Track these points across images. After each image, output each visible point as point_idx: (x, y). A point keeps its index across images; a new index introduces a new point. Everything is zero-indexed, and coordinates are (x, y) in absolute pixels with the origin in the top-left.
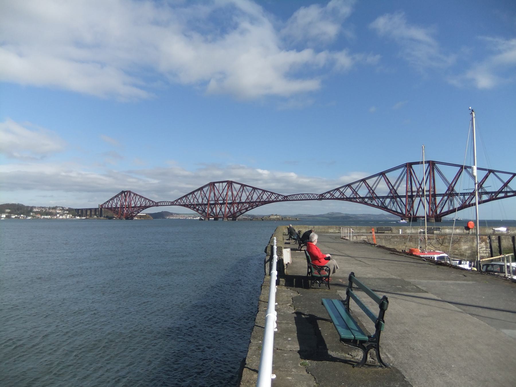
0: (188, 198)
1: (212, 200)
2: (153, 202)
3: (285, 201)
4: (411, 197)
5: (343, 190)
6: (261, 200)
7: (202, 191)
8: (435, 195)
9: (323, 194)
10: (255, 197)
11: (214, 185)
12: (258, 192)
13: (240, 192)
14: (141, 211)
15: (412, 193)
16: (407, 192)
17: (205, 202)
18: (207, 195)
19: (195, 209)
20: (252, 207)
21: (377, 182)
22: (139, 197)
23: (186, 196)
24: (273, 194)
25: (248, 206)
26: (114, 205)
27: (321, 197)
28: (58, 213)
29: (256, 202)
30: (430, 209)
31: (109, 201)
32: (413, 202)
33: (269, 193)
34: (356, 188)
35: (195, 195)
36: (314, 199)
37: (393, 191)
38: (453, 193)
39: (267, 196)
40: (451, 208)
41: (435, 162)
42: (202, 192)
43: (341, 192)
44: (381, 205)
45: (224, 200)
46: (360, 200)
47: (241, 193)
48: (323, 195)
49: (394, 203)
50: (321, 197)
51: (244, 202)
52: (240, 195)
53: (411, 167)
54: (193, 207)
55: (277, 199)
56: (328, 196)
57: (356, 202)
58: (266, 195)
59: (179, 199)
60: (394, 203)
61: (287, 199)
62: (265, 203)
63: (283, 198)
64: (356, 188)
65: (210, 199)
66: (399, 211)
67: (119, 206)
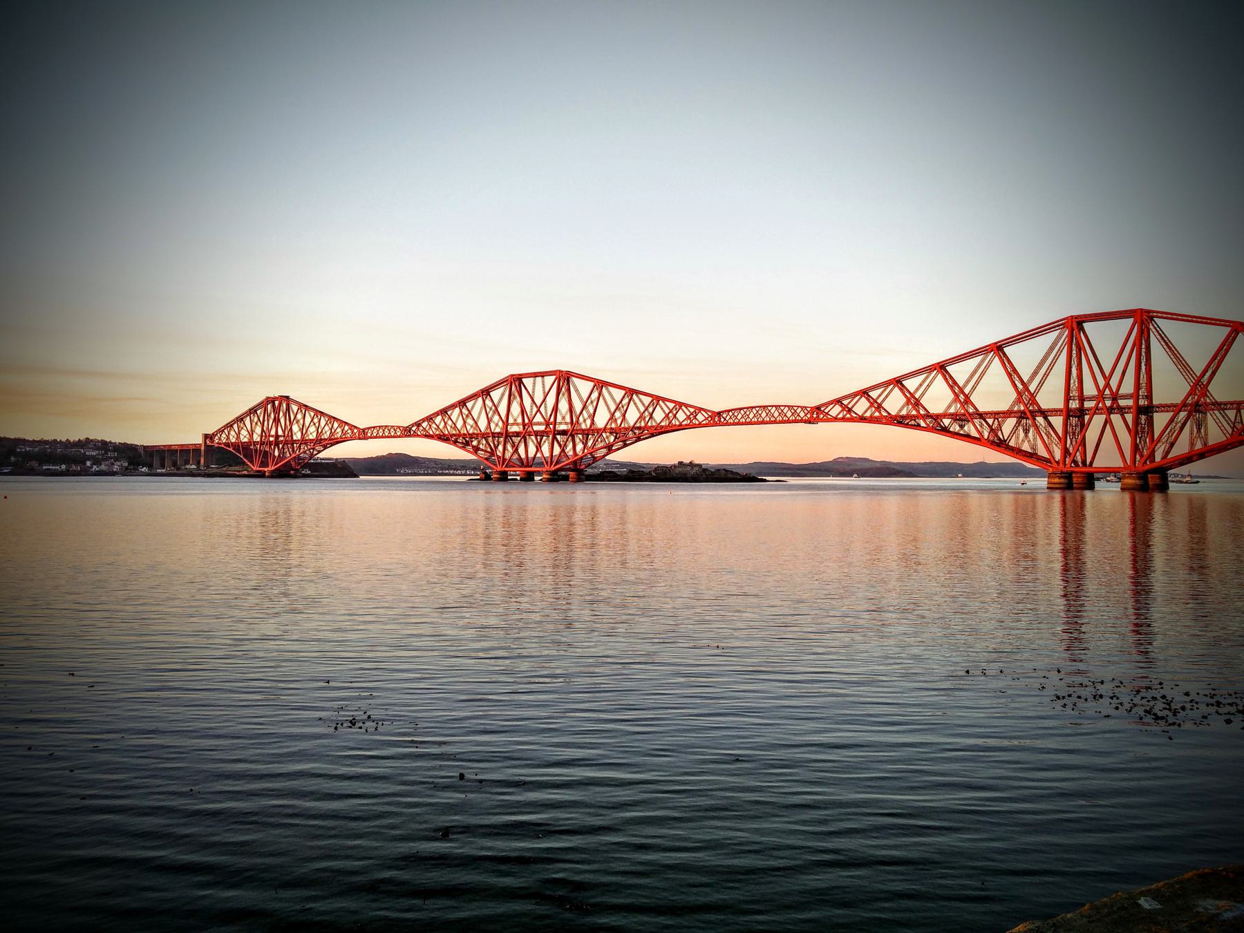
0: (450, 418)
1: (515, 423)
2: (352, 427)
3: (715, 425)
4: (1081, 412)
5: (880, 396)
6: (649, 424)
7: (486, 398)
8: (1147, 411)
9: (823, 405)
10: (632, 417)
11: (521, 382)
12: (641, 401)
13: (592, 402)
14: (319, 452)
15: (1082, 404)
16: (1068, 398)
17: (495, 429)
18: (503, 409)
19: (469, 448)
21: (978, 375)
22: (312, 414)
23: (444, 412)
24: (680, 408)
25: (612, 439)
26: (245, 437)
27: (815, 416)
28: (89, 458)
29: (633, 428)
30: (1135, 449)
31: (231, 426)
32: (1083, 427)
33: (671, 405)
34: (917, 389)
36: (796, 421)
37: (1026, 397)
38: (1206, 403)
39: (664, 411)
40: (1199, 446)
41: (1155, 314)
42: (488, 402)
43: (872, 400)
44: (988, 437)
45: (547, 424)
46: (928, 421)
47: (595, 404)
48: (822, 409)
49: (1026, 431)
50: (815, 416)
51: (600, 429)
52: (591, 409)
53: (1082, 329)
54: (464, 441)
55: (691, 421)
56: (835, 411)
57: (918, 427)
58: (662, 409)
59: (423, 420)
60: (1026, 431)
61: (720, 420)
63: (710, 416)
64: (917, 389)
65: (511, 421)
66: (1042, 452)
67: (256, 438)
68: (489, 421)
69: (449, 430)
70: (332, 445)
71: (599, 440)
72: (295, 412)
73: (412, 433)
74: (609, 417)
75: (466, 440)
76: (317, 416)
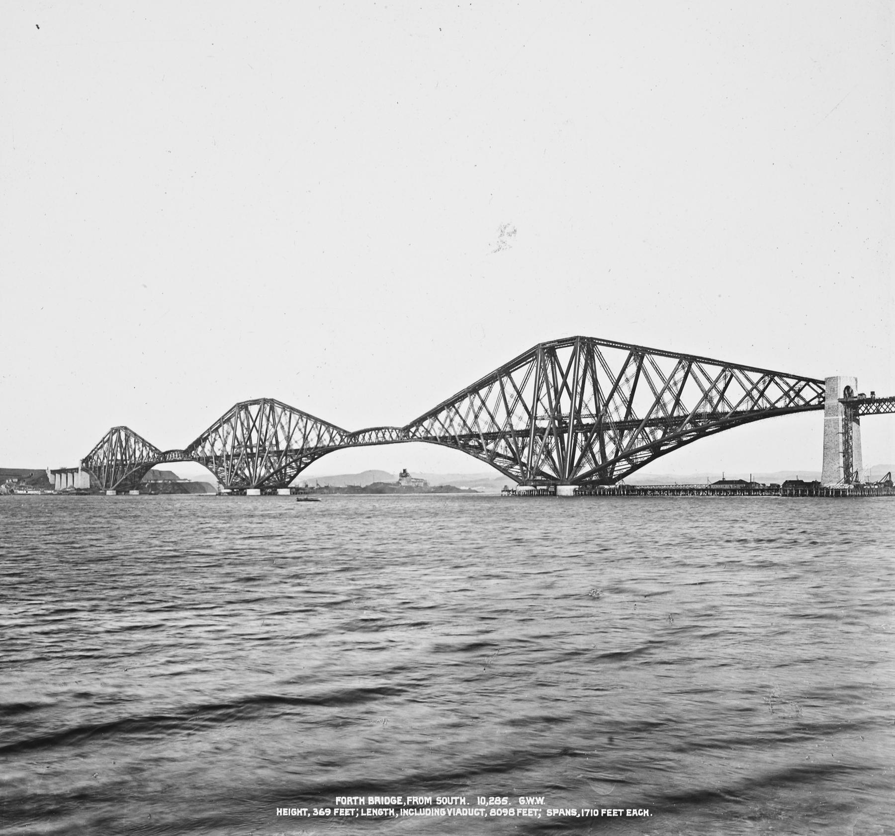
0: (457, 412)
10: (691, 399)
13: (627, 380)
14: (307, 465)
18: (528, 396)
20: (678, 437)
22: (297, 417)
25: (659, 434)
29: (696, 416)
33: (755, 377)
35: (483, 397)
52: (626, 390)
62: (739, 418)
68: (509, 413)
69: (456, 429)
70: (320, 456)
71: (640, 436)
72: (279, 414)
73: (411, 434)
74: (654, 399)
75: (479, 443)
76: (302, 420)
